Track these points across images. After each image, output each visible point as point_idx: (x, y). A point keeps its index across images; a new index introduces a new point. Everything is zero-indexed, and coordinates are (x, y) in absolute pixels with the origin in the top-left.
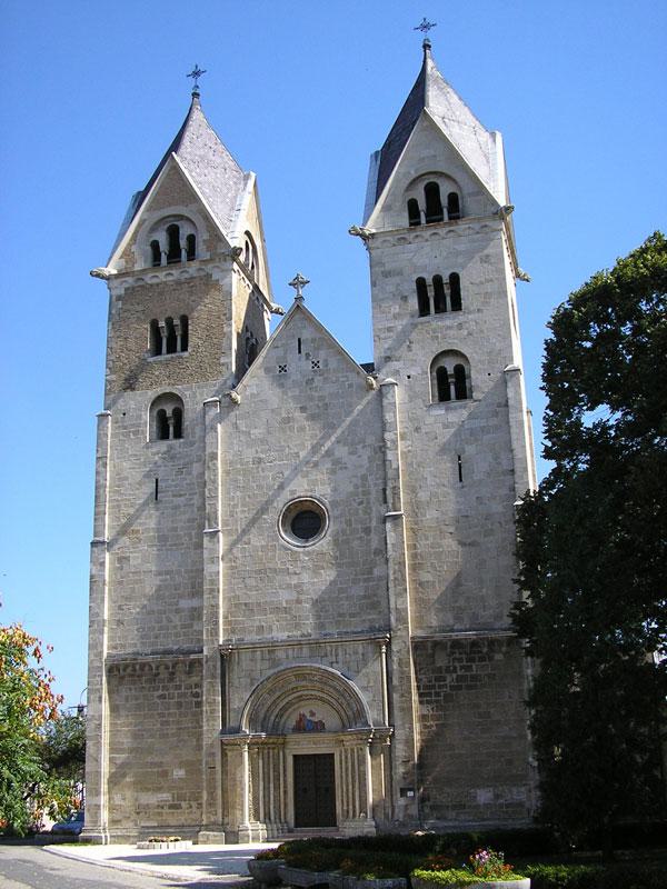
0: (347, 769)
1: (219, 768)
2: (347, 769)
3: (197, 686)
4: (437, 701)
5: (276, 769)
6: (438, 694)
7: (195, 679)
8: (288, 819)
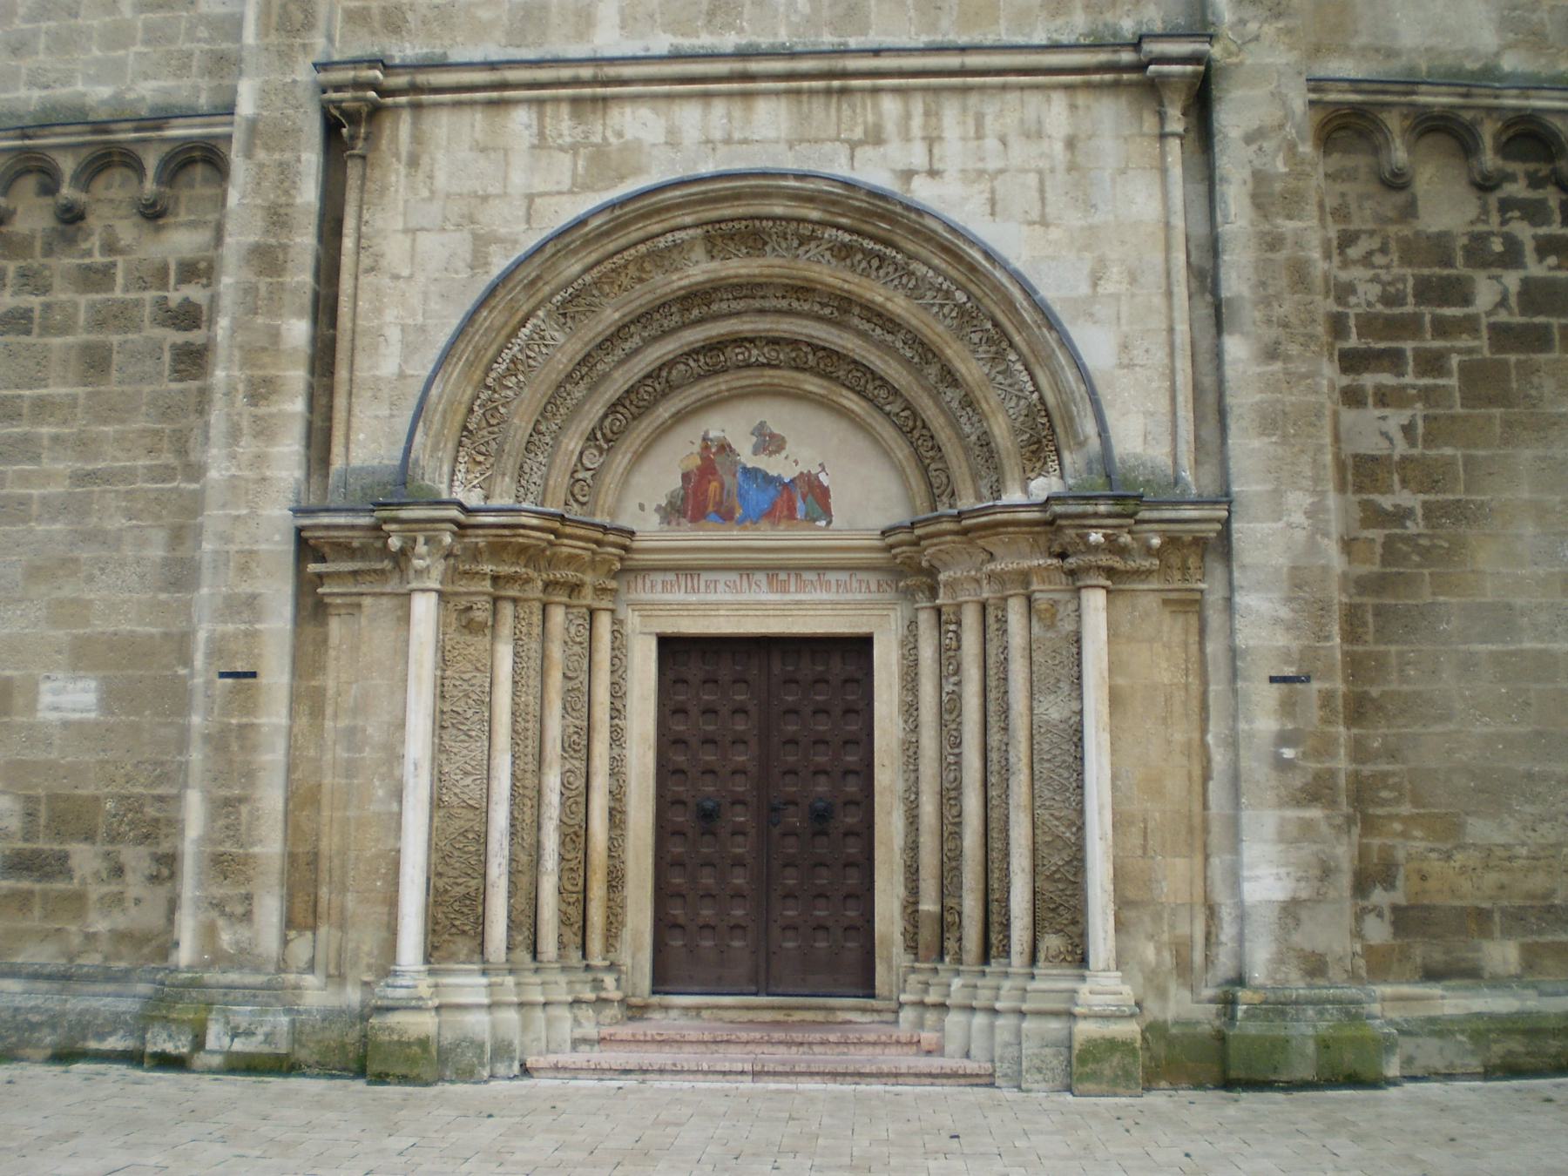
0: (950, 708)
1: (276, 676)
2: (950, 708)
3: (190, 271)
4: (1426, 394)
5: (579, 700)
6: (1432, 363)
7: (180, 241)
8: (625, 957)
